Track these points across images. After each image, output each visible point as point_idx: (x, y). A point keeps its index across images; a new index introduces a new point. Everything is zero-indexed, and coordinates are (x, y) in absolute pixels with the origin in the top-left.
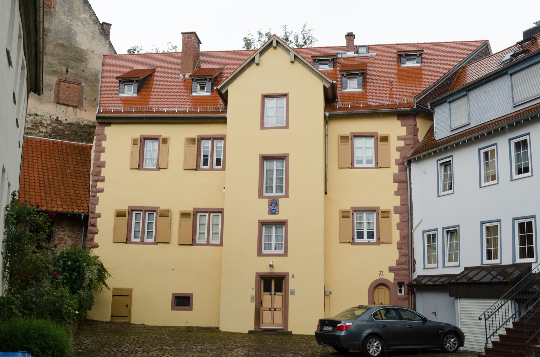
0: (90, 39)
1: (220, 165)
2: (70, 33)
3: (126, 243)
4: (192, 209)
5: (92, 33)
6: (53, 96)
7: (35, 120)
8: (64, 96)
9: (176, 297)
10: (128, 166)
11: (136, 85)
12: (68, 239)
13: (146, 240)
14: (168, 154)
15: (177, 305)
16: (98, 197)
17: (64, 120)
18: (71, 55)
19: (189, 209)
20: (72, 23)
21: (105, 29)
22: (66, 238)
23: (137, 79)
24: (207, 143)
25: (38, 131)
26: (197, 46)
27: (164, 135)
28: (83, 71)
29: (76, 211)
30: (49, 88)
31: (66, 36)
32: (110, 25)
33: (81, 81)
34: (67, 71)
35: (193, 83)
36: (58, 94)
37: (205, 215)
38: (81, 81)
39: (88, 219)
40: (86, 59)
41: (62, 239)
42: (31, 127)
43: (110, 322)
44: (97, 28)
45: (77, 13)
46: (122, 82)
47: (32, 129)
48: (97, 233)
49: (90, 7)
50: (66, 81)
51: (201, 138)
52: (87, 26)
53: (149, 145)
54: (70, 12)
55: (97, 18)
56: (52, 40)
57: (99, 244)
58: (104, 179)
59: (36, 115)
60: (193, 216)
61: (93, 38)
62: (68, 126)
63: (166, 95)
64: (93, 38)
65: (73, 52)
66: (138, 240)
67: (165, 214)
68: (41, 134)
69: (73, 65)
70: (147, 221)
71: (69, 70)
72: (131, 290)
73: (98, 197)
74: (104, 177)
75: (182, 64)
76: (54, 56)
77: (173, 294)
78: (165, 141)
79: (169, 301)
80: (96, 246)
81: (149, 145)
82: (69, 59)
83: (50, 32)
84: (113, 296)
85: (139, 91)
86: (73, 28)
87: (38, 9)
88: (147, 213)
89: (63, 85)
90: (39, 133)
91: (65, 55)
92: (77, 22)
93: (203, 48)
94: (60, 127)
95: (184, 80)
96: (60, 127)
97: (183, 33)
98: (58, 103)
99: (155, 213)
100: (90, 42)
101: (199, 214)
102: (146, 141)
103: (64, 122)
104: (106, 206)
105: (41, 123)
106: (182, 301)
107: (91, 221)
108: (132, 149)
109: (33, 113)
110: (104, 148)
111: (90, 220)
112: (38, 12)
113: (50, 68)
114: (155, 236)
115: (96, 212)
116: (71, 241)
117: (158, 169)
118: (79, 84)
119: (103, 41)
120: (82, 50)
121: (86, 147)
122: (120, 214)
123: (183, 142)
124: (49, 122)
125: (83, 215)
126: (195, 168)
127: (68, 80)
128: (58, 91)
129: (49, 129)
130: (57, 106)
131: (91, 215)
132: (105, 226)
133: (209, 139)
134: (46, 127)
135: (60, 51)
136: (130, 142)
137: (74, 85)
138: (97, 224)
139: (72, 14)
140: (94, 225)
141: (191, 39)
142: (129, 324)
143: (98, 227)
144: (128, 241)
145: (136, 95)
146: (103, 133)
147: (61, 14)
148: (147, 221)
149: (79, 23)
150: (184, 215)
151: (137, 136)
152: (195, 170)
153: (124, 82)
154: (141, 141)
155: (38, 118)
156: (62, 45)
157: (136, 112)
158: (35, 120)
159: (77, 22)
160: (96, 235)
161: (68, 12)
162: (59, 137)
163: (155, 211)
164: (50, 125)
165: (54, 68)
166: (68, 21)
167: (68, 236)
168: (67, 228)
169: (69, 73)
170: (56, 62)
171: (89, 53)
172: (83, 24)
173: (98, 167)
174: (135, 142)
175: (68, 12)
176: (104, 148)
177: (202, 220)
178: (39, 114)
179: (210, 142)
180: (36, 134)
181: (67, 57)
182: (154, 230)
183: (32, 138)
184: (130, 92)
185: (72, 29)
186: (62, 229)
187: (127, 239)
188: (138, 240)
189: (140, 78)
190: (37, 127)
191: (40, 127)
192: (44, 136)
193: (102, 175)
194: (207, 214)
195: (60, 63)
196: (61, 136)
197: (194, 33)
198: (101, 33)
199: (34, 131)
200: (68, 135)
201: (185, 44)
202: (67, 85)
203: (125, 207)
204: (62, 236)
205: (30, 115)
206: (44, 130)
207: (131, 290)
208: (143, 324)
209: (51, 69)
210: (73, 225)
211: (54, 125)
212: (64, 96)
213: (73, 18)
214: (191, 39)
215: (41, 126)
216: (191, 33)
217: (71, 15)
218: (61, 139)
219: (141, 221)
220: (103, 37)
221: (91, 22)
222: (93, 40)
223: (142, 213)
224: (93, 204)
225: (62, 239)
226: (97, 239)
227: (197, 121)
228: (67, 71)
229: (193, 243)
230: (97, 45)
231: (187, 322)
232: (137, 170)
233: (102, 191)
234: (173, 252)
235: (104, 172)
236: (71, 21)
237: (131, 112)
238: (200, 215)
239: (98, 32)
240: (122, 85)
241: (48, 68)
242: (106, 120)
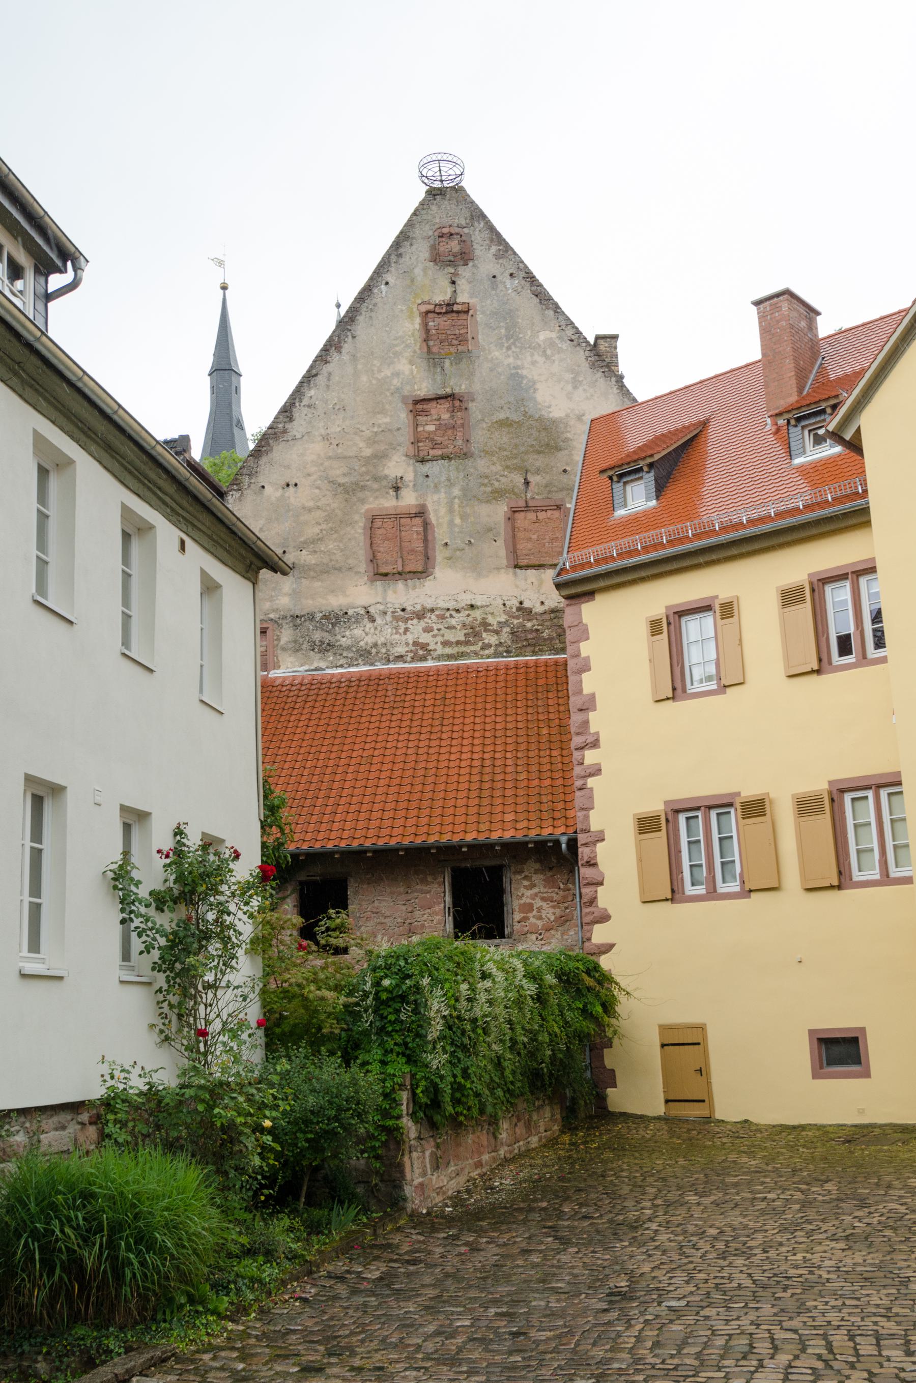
0: (569, 387)
1: (850, 652)
2: (519, 387)
3: (672, 900)
4: (826, 786)
5: (572, 371)
6: (503, 553)
7: (470, 619)
8: (529, 546)
9: (821, 1040)
10: (648, 697)
11: (649, 478)
12: (544, 905)
13: (722, 888)
14: (740, 643)
15: (830, 1063)
16: (591, 789)
17: (539, 604)
18: (531, 441)
19: (819, 785)
20: (519, 363)
21: (602, 354)
22: (538, 903)
23: (649, 460)
24: (842, 591)
25: (480, 644)
26: (803, 324)
27: (724, 595)
28: (565, 471)
29: (546, 832)
30: (490, 535)
31: (512, 399)
32: (615, 337)
33: (562, 500)
34: (527, 483)
35: (792, 430)
36: (514, 546)
37: (866, 798)
38: (562, 500)
39: (577, 848)
40: (566, 440)
41: (529, 908)
42: (462, 638)
43: (665, 1119)
44: (581, 356)
45: (529, 333)
46: (615, 479)
47: (467, 643)
48: (602, 884)
49: (557, 308)
50: (527, 508)
51: (822, 582)
52: (556, 357)
53: (697, 629)
54: (512, 337)
55: (578, 332)
56: (480, 417)
57: (610, 912)
58: (597, 740)
59: (472, 606)
60: (830, 804)
61: (576, 384)
62: (547, 617)
63: (741, 482)
64: (576, 384)
65: (535, 433)
66: (701, 890)
67: (756, 808)
68: (487, 652)
69: (538, 464)
70: (715, 836)
71: (530, 478)
72: (702, 1028)
73: (591, 789)
74: (597, 733)
75: (766, 386)
76: (492, 454)
77: (811, 1032)
78: (728, 610)
79: (802, 1054)
80: (604, 918)
81: (697, 629)
82: (526, 453)
83: (473, 400)
84: (663, 1046)
85: (660, 490)
86: (524, 372)
87: (80, 384)
88: (713, 814)
89: (522, 520)
90: (482, 649)
91: (516, 446)
92: (532, 355)
93: (825, 327)
94: (529, 625)
95: (774, 429)
96: (529, 625)
97: (757, 303)
98: (517, 566)
99: (732, 811)
100: (569, 397)
101: (848, 797)
102: (684, 620)
103: (539, 609)
104: (612, 811)
105: (485, 624)
106: (840, 1051)
107: (584, 853)
108: (651, 649)
109: (463, 605)
110: (587, 659)
111: (580, 850)
112: (86, 391)
113: (485, 485)
114: (741, 875)
115: (592, 830)
116: (552, 910)
117: (724, 688)
118: (559, 507)
119: (602, 382)
120: (554, 421)
121: (556, 663)
122: (646, 825)
123: (774, 601)
124: (503, 618)
125: (564, 839)
126: (816, 668)
127: (531, 504)
128: (514, 536)
129: (505, 636)
130: (515, 574)
131: (582, 839)
132: (617, 860)
133: (843, 577)
134: (497, 632)
135: (503, 438)
136: (644, 630)
137: (549, 512)
138: (600, 860)
139: (518, 339)
140: (592, 864)
141: (786, 314)
142: (708, 1119)
143: (602, 866)
144: (675, 895)
145: (654, 503)
146: (581, 622)
147: (493, 347)
148: (715, 836)
149: (537, 357)
150: (806, 806)
151: (658, 610)
152: (818, 672)
153: (621, 476)
154: (669, 624)
155: (477, 614)
156: (504, 424)
157: (646, 549)
158: (470, 619)
159: (532, 355)
160: (600, 889)
161: (508, 339)
162: (529, 649)
163: (731, 805)
164: (506, 623)
165: (496, 484)
166: (511, 360)
167: (543, 899)
168: (538, 879)
169: (532, 486)
170: (498, 468)
171: (572, 423)
172: (547, 357)
173: (581, 710)
174: (655, 627)
175: (508, 339)
176: (587, 659)
177: (860, 813)
178: (479, 604)
179: (848, 584)
180: (476, 654)
181: (522, 449)
182: (737, 858)
183: (468, 666)
184: (638, 498)
185: (522, 377)
186: (526, 883)
187: (673, 891)
188: (701, 890)
189: (657, 457)
190: (477, 635)
191: (484, 635)
192: (497, 655)
193: (593, 730)
194: (870, 794)
195: (507, 467)
196: (534, 645)
197: (787, 292)
198: (593, 366)
199: (472, 648)
200: (551, 639)
201: (766, 331)
202: (531, 516)
203: (655, 806)
204: (529, 901)
205: (458, 611)
206: (492, 639)
207: (702, 1028)
208: (746, 1121)
209: (489, 489)
210: (551, 869)
211: (515, 622)
212: (529, 546)
213: (521, 348)
214: (786, 314)
215: (485, 631)
216: (778, 295)
217: (514, 343)
218: (534, 653)
219: (701, 838)
220: (600, 374)
221: (565, 345)
222: (575, 388)
223: (699, 814)
224: (582, 809)
225: (529, 908)
226: (605, 898)
227: (814, 531)
228: (527, 483)
229: (843, 880)
230: (587, 398)
231: (861, 1112)
232: (670, 702)
233: (596, 771)
234: (793, 913)
235: (597, 721)
236: (517, 357)
237: (636, 552)
238: (853, 800)
239: (585, 365)
240: (618, 487)
241: (482, 488)
242: (578, 589)
